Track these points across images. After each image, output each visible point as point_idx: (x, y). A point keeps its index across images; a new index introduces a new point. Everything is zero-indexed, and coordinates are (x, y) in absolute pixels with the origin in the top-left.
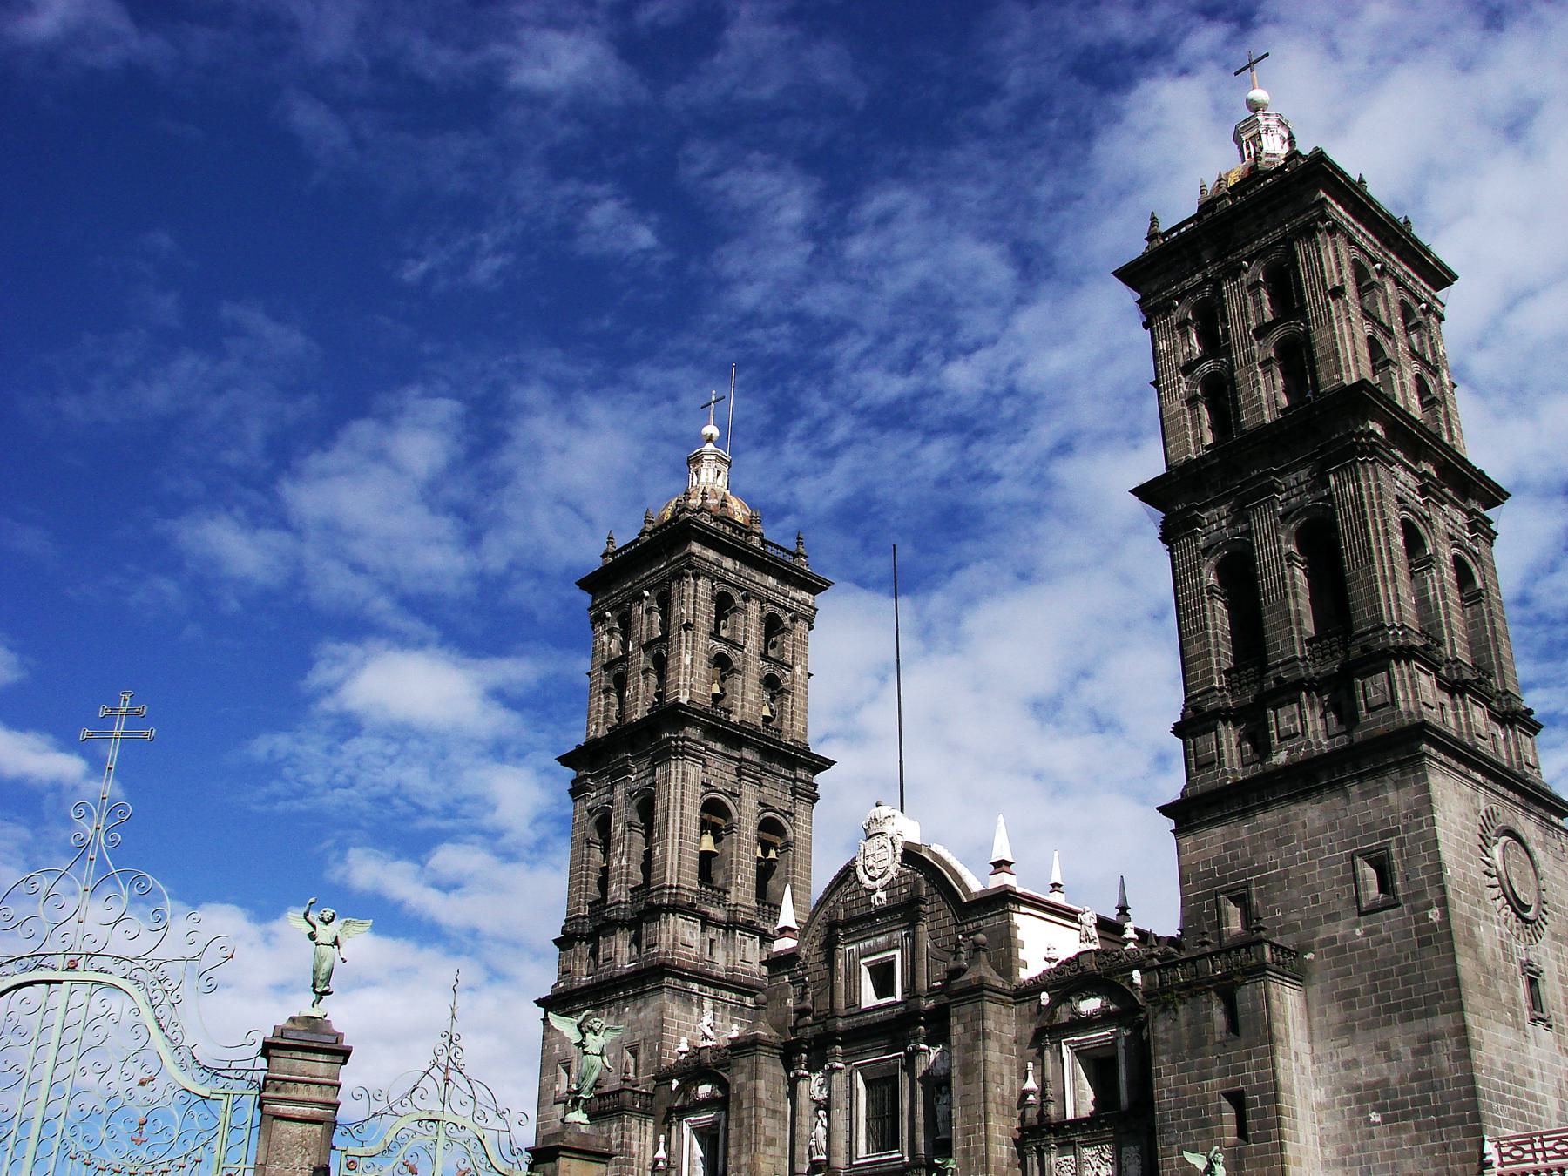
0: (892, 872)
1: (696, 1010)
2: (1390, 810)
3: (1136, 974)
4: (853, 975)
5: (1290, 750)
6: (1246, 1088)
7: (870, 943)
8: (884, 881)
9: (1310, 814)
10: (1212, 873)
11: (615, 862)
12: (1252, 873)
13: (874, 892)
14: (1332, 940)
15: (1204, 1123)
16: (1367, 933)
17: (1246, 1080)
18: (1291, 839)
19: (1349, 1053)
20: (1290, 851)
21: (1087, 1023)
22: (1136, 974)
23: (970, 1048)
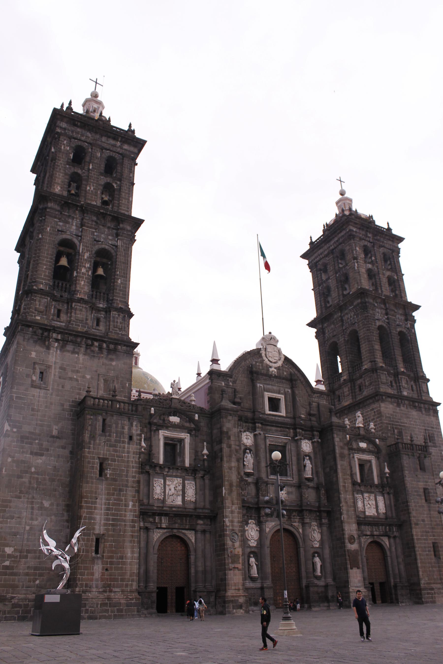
0: (280, 363)
2: (432, 421)
3: (377, 440)
4: (263, 397)
5: (408, 393)
6: (429, 488)
7: (270, 387)
8: (276, 365)
9: (414, 413)
10: (390, 418)
11: (83, 270)
12: (401, 423)
13: (271, 367)
15: (419, 495)
17: (429, 486)
20: (410, 421)
21: (362, 451)
22: (377, 440)
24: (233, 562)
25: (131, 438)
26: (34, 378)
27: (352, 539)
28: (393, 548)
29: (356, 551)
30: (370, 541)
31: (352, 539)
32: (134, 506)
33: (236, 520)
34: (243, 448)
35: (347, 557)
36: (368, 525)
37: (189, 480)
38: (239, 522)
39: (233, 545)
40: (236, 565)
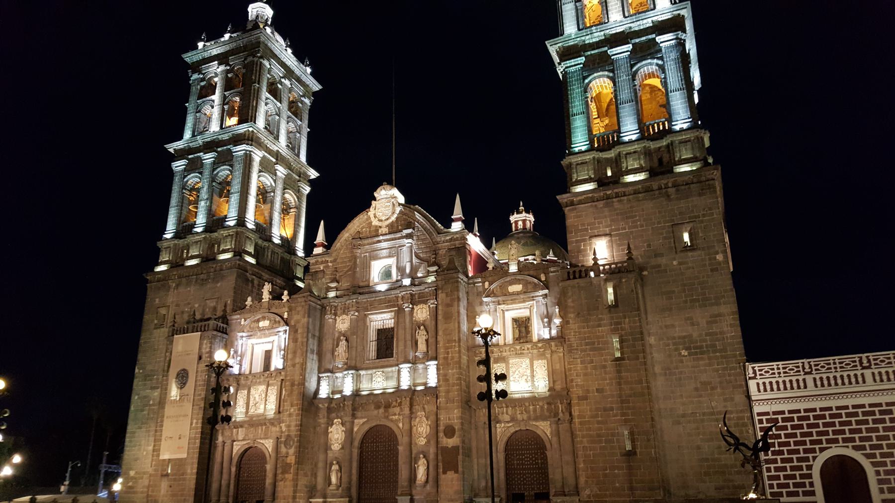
1: (250, 284)
14: (659, 266)
16: (680, 264)
17: (622, 329)
18: (636, 216)
19: (669, 322)
23: (449, 305)
24: (284, 472)
25: (200, 358)
26: (156, 322)
27: (450, 432)
28: (555, 440)
29: (455, 449)
30: (512, 430)
31: (450, 432)
32: (197, 423)
33: (293, 424)
34: (337, 335)
35: (440, 457)
36: (507, 407)
37: (273, 385)
38: (296, 426)
39: (287, 453)
40: (287, 476)
